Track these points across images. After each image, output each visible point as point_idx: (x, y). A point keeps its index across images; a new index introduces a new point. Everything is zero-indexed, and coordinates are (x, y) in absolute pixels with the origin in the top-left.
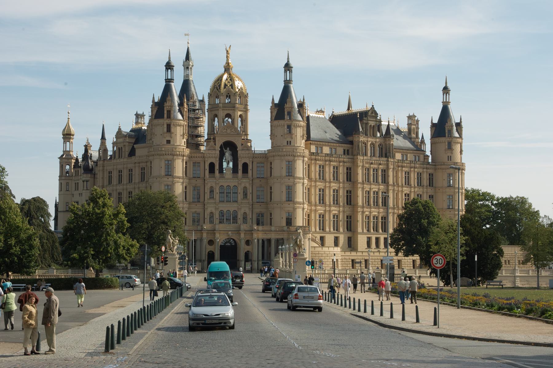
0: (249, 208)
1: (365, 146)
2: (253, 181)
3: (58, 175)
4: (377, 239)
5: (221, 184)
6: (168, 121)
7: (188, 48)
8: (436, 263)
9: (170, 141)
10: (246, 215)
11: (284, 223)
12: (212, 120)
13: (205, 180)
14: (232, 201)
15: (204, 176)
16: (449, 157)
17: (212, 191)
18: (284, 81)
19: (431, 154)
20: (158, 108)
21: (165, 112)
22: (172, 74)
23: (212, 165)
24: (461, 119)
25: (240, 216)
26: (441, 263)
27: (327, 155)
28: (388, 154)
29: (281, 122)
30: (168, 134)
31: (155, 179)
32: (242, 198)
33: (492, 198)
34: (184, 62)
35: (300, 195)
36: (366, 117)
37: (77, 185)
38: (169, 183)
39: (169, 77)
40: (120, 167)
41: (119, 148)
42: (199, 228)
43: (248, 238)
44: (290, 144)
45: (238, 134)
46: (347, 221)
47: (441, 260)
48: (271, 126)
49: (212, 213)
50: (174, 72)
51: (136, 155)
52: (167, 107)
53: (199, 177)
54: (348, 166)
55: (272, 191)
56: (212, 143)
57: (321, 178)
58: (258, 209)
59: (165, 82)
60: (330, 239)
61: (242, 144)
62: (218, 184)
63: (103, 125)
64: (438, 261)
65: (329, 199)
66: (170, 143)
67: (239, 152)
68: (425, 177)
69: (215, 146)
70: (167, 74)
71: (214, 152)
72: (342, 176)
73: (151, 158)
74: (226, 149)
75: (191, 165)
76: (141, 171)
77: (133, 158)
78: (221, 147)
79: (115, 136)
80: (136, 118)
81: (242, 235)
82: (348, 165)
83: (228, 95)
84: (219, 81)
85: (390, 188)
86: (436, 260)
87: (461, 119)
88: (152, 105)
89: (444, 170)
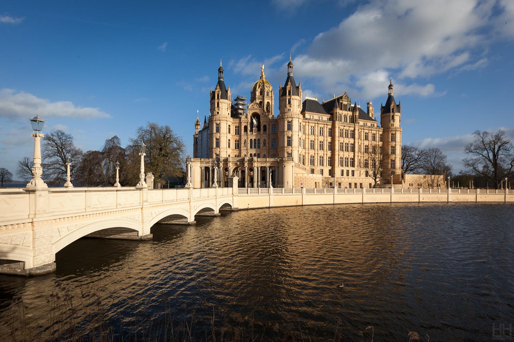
1: (341, 117)
2: (270, 136)
4: (348, 171)
19: (381, 124)
23: (246, 127)
24: (400, 102)
27: (316, 120)
29: (284, 97)
33: (416, 149)
44: (290, 111)
57: (312, 134)
61: (263, 114)
65: (317, 146)
67: (261, 119)
71: (246, 119)
74: (254, 118)
85: (357, 141)
87: (400, 102)
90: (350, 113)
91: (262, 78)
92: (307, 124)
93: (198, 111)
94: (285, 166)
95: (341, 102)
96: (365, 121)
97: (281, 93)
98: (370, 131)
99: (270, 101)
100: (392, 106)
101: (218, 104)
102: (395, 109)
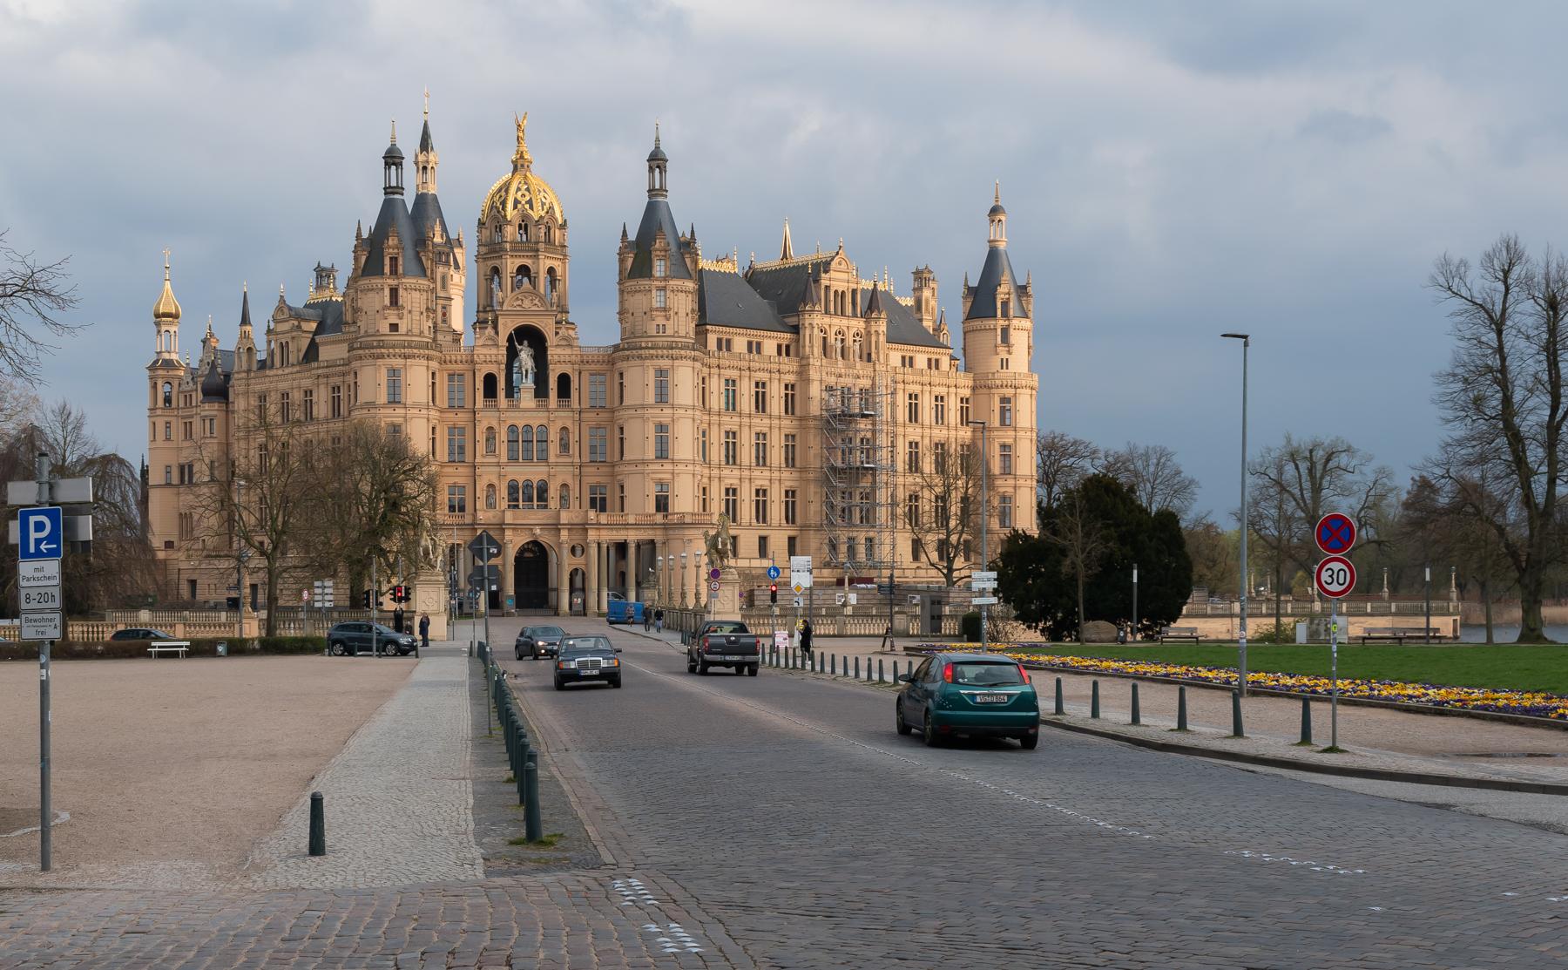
2: (582, 415)
5: (510, 422)
6: (393, 282)
8: (1329, 580)
9: (397, 325)
10: (568, 490)
11: (651, 508)
12: (486, 279)
13: (475, 412)
14: (535, 460)
15: (471, 406)
16: (1005, 361)
18: (649, 191)
20: (370, 253)
21: (387, 261)
22: (399, 177)
23: (490, 381)
25: (553, 492)
26: (1341, 581)
28: (873, 356)
29: (644, 282)
31: (366, 411)
32: (558, 452)
34: (417, 156)
35: (684, 445)
36: (826, 272)
37: (188, 427)
38: (397, 419)
39: (394, 184)
40: (283, 386)
41: (281, 343)
42: (468, 520)
43: (577, 539)
46: (787, 502)
47: (1342, 573)
48: (622, 292)
49: (491, 486)
50: (404, 170)
51: (320, 359)
53: (462, 407)
54: (788, 382)
55: (624, 436)
56: (490, 331)
57: (731, 408)
58: (593, 476)
59: (385, 194)
60: (749, 542)
61: (557, 333)
63: (245, 293)
64: (1335, 576)
65: (746, 454)
66: (397, 331)
68: (953, 406)
70: (387, 177)
71: (494, 351)
72: (776, 404)
73: (355, 364)
74: (521, 344)
75: (442, 382)
76: (330, 395)
77: (314, 365)
78: (510, 339)
79: (273, 316)
80: (317, 278)
81: (564, 534)
82: (790, 378)
83: (523, 224)
84: (503, 193)
86: (1330, 572)
88: (355, 246)
89: (993, 391)
90: (858, 324)
91: (522, 166)
92: (715, 371)
94: (690, 540)
95: (827, 283)
96: (908, 350)
97: (630, 262)
98: (927, 388)
99: (556, 264)
100: (1003, 291)
101: (394, 292)
102: (1011, 305)
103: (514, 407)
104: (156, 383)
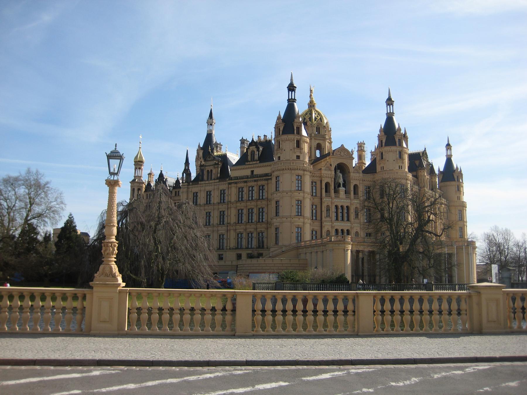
0: (360, 228)
3: (129, 197)
5: (336, 204)
6: (297, 137)
7: (211, 110)
17: (328, 210)
21: (295, 128)
30: (297, 150)
38: (300, 198)
40: (208, 188)
41: (208, 171)
45: (350, 157)
49: (328, 231)
52: (297, 124)
59: (288, 102)
62: (334, 203)
66: (299, 159)
69: (330, 166)
71: (329, 172)
83: (318, 127)
93: (141, 137)
103: (337, 197)
104: (134, 189)
